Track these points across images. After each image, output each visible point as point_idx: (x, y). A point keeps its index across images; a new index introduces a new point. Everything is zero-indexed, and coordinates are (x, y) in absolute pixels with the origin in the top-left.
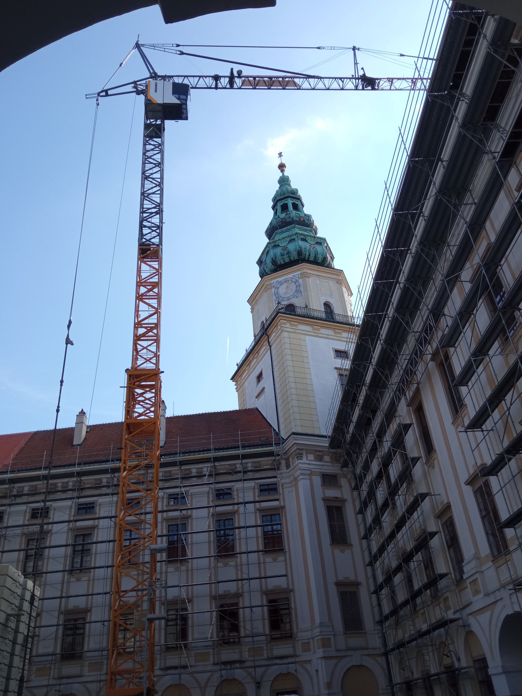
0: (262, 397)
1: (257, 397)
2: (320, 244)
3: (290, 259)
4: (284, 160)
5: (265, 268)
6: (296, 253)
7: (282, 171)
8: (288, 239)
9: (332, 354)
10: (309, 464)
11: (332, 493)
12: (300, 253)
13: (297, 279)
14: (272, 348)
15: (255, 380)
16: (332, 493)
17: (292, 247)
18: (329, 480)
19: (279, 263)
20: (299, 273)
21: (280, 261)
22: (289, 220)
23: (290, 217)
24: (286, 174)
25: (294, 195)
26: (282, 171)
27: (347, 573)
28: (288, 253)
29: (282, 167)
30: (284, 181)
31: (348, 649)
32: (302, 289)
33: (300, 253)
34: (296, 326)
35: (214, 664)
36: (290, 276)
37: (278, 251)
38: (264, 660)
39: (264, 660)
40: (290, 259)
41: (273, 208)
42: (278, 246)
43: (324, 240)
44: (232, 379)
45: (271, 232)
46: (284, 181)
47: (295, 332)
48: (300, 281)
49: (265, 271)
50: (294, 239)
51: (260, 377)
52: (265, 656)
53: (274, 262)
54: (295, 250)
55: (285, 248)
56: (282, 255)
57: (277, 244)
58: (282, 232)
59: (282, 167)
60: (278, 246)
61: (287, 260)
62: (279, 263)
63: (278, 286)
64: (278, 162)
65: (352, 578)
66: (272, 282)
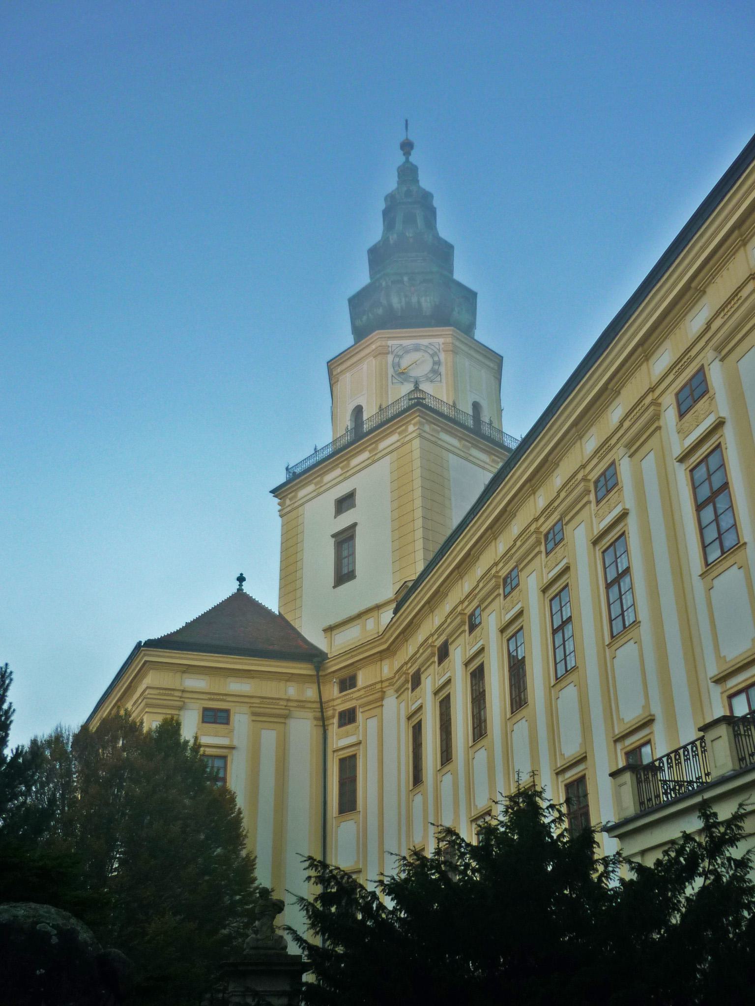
7: (407, 154)
25: (425, 201)
26: (407, 154)
32: (443, 369)
36: (425, 342)
48: (442, 356)
51: (345, 503)
63: (400, 353)
66: (390, 343)
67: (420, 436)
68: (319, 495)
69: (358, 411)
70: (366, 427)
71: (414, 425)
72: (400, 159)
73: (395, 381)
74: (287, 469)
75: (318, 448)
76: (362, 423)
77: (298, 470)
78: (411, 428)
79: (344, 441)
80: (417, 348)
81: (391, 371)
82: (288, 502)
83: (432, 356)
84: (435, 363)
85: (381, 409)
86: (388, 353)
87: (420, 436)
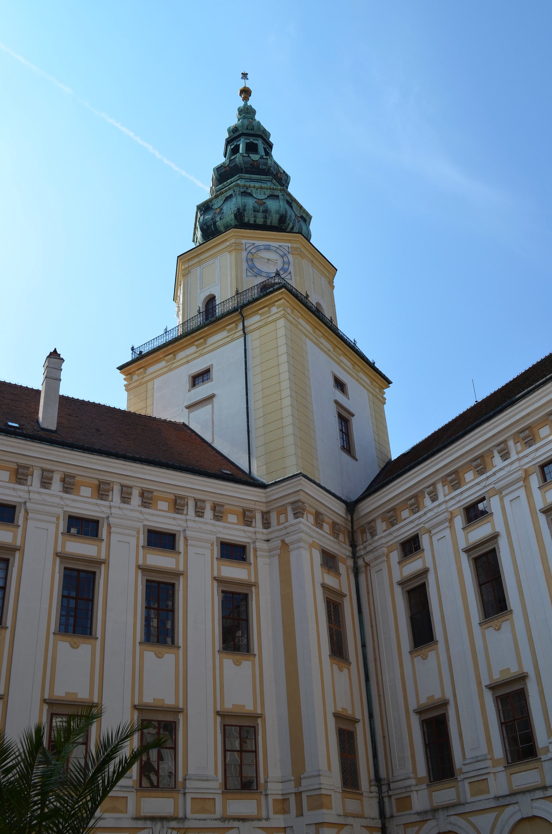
0: (206, 410)
1: (188, 407)
2: (305, 221)
3: (265, 222)
4: (249, 84)
5: (218, 219)
6: (278, 216)
7: (246, 99)
8: (268, 192)
9: (332, 381)
10: (310, 528)
11: (331, 581)
12: (283, 218)
13: (287, 253)
14: (249, 337)
15: (186, 382)
16: (331, 581)
17: (272, 205)
18: (329, 561)
19: (246, 220)
20: (289, 245)
21: (249, 217)
22: (264, 167)
23: (266, 164)
24: (249, 103)
26: (246, 99)
27: (344, 704)
28: (266, 211)
29: (246, 93)
30: (247, 113)
31: (346, 815)
32: (291, 269)
33: (283, 218)
34: (298, 319)
35: (137, 819)
36: (276, 244)
37: (250, 202)
38: (216, 819)
39: (216, 819)
40: (265, 222)
41: (229, 142)
42: (250, 195)
43: (310, 218)
44: (120, 368)
45: (222, 175)
46: (247, 113)
47: (296, 326)
48: (290, 257)
49: (215, 223)
50: (278, 196)
51: (202, 377)
52: (219, 813)
53: (239, 215)
54: (278, 212)
55: (261, 202)
56: (255, 210)
57: (249, 191)
58: (251, 180)
59: (246, 93)
60: (250, 195)
61: (260, 221)
62: (246, 220)
64: (242, 84)
65: (350, 712)
66: (244, 241)
67: (284, 316)
68: (170, 370)
69: (211, 300)
70: (219, 311)
71: (278, 307)
72: (241, 103)
73: (249, 274)
74: (133, 349)
75: (168, 330)
76: (214, 307)
77: (145, 350)
78: (274, 309)
79: (193, 325)
80: (268, 248)
81: (245, 266)
82: (135, 377)
83: (282, 257)
84: (284, 263)
85: (237, 293)
86: (242, 250)
87: (284, 316)
